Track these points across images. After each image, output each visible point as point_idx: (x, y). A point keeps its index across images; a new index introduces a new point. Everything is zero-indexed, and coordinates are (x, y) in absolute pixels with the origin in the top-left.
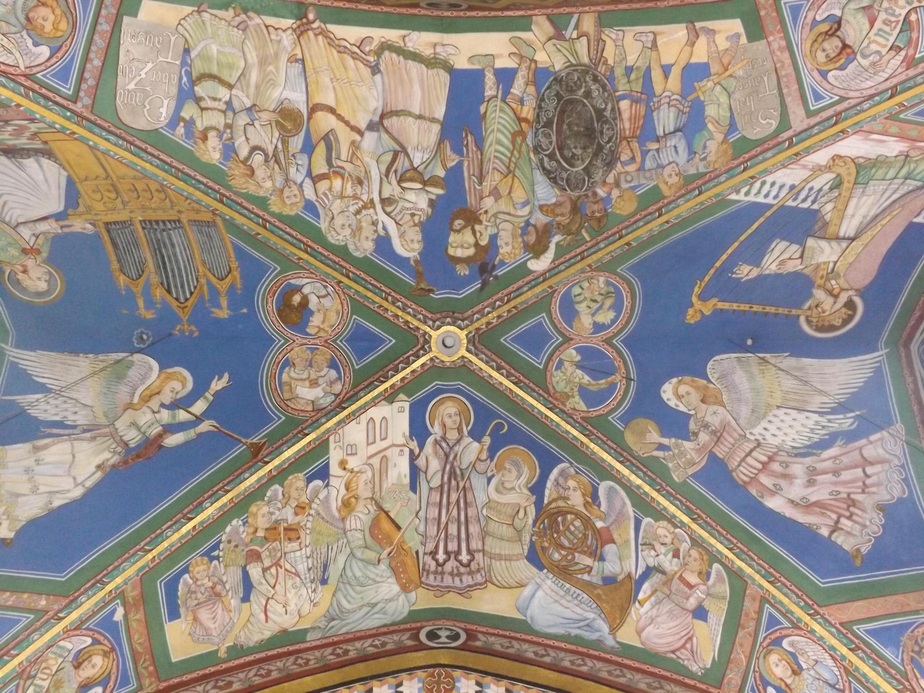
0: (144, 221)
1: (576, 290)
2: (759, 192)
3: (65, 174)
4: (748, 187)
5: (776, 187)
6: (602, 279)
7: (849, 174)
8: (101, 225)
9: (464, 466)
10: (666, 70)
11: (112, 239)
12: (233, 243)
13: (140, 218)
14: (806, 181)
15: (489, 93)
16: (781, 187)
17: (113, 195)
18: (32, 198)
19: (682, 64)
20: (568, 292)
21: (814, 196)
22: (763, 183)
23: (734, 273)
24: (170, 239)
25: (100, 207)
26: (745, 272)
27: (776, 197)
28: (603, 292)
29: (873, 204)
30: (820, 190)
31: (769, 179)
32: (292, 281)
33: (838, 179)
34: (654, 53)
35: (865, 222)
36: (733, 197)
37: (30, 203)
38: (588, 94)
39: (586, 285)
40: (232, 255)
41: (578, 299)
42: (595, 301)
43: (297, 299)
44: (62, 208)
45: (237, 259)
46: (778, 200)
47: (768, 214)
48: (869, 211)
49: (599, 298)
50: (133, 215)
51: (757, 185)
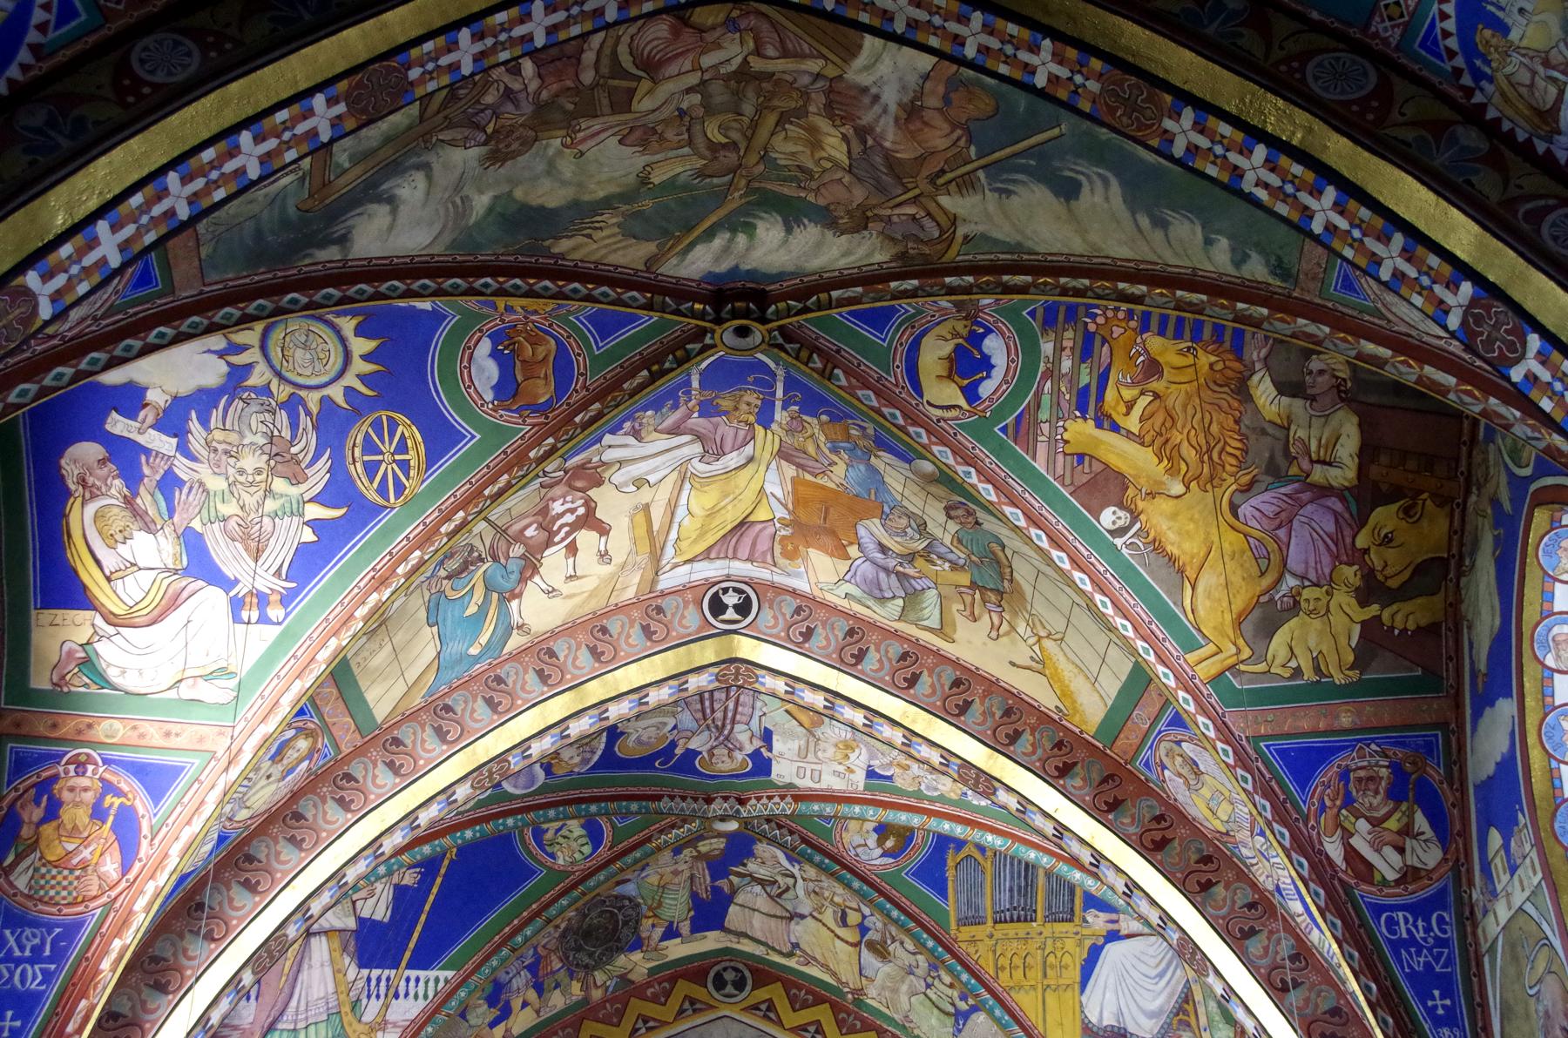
0: (1031, 921)
1: (587, 850)
2: (427, 983)
3: (1084, 999)
4: (439, 988)
5: (412, 993)
6: (561, 862)
7: (351, 1025)
8: (1077, 920)
9: (707, 733)
10: (525, 1004)
11: (1073, 901)
12: (946, 898)
13: (1034, 924)
14: (387, 1006)
15: (688, 923)
16: (407, 995)
17: (1051, 959)
18: (1129, 967)
19: (512, 1018)
20: (595, 849)
21: (372, 988)
22: (426, 997)
23: (420, 873)
24: (1012, 897)
25: (1070, 944)
26: (407, 876)
27: (408, 980)
28: (558, 847)
29: (309, 987)
30: (369, 997)
31: (421, 1003)
32: (891, 860)
33: (358, 1016)
34: (537, 1006)
35: (306, 960)
36: (450, 974)
37: (1135, 961)
38: (591, 955)
39: (578, 856)
40: (950, 884)
41: (584, 840)
42: (565, 837)
43: (889, 844)
44: (1108, 946)
45: (946, 879)
46: (404, 977)
47: (408, 955)
48: (309, 974)
49: (560, 840)
50: (1041, 929)
51: (431, 994)
